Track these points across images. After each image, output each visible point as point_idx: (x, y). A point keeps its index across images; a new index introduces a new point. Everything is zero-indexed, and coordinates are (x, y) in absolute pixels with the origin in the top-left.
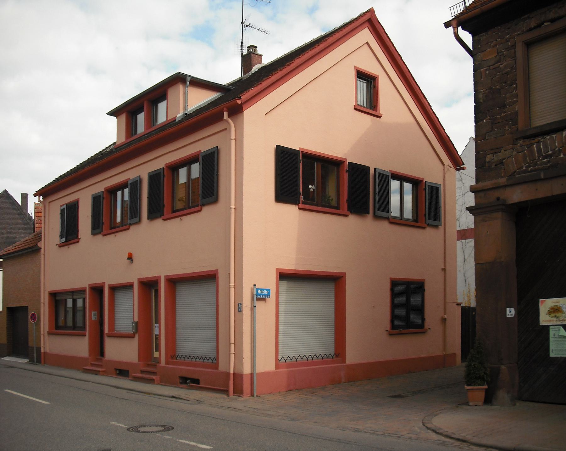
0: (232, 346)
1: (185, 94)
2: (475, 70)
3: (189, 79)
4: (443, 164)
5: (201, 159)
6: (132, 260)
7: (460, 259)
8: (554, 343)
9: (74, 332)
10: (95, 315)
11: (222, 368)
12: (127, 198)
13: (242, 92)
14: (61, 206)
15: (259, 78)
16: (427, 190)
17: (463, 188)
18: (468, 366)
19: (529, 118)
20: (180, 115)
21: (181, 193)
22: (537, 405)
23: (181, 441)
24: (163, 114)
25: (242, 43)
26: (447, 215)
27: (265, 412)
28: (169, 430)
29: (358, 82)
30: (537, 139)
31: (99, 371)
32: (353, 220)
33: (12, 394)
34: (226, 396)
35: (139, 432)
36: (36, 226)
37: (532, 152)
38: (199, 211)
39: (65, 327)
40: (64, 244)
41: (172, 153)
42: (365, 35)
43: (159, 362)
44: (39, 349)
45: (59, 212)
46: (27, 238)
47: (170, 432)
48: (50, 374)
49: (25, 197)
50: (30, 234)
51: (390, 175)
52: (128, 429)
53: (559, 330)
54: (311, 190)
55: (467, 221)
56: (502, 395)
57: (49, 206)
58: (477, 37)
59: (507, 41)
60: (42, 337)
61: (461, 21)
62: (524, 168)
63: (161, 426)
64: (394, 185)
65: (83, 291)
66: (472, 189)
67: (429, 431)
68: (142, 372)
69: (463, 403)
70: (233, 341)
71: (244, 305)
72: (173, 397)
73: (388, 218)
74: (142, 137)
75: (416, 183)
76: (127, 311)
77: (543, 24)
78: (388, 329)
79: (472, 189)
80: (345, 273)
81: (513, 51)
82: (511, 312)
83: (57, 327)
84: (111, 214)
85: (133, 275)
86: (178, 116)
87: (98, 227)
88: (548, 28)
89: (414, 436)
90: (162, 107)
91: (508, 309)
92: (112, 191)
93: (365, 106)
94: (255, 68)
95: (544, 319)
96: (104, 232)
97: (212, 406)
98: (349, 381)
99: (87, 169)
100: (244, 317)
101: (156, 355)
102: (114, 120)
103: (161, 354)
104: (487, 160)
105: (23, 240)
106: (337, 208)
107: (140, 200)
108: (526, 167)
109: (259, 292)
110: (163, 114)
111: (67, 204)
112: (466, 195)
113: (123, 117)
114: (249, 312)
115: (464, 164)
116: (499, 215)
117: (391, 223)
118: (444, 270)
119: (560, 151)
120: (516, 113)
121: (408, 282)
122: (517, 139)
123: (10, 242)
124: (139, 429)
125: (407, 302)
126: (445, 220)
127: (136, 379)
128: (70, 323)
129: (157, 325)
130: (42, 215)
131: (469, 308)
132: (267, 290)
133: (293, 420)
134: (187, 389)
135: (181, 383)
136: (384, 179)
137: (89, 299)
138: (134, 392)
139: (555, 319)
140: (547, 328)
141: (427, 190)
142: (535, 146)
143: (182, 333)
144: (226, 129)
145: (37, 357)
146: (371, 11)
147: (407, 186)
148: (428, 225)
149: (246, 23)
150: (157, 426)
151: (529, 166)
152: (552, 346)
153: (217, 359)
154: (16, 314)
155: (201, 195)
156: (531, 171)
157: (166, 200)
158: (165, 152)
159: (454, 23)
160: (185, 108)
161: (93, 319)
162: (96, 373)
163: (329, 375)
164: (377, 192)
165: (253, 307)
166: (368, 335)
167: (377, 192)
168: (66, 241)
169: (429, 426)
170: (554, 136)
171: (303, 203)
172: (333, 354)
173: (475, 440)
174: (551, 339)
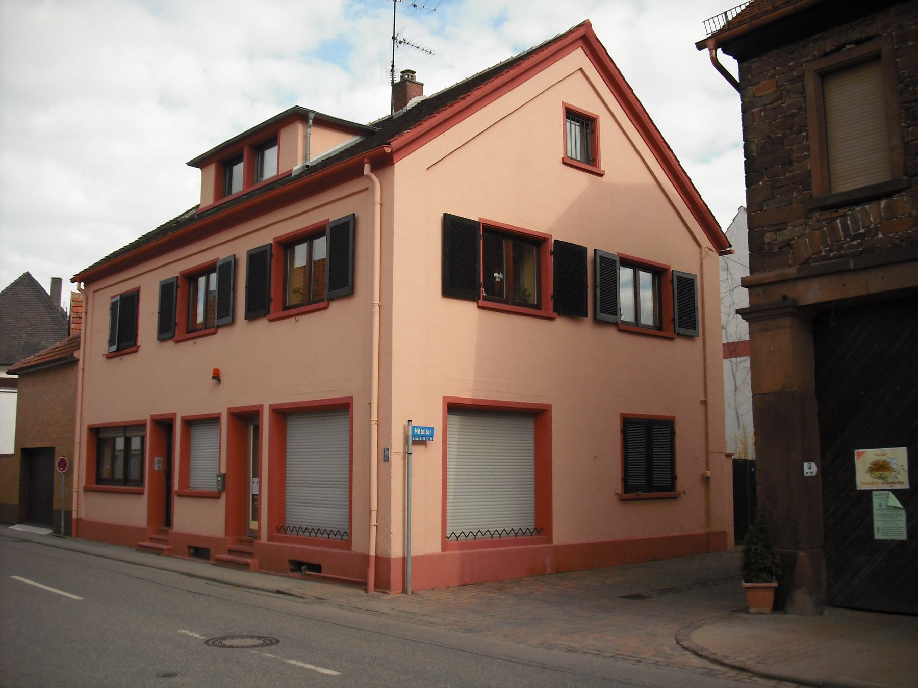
0: (374, 514)
1: (306, 137)
2: (744, 111)
3: (312, 116)
4: (699, 245)
5: (328, 232)
6: (219, 380)
7: (728, 386)
8: (880, 518)
9: (126, 487)
10: (159, 462)
11: (357, 547)
12: (213, 286)
13: (392, 136)
14: (112, 297)
15: (417, 116)
16: (675, 283)
17: (730, 280)
18: (747, 552)
19: (828, 180)
20: (297, 167)
21: (297, 282)
22: (857, 614)
23: (290, 662)
24: (272, 165)
25: (393, 66)
26: (707, 321)
27: (425, 618)
28: (271, 643)
29: (568, 124)
30: (841, 212)
31: (163, 550)
32: (561, 326)
33: (24, 583)
34: (362, 592)
35: (224, 646)
36: (73, 326)
37: (834, 229)
38: (325, 308)
39: (112, 480)
40: (115, 354)
41: (285, 222)
42: (578, 58)
43: (258, 537)
44: (69, 513)
45: (109, 306)
46: (58, 344)
47: (273, 647)
48: (85, 553)
49: (57, 283)
50: (63, 338)
51: (618, 260)
52: (206, 642)
53: (888, 497)
54: (498, 280)
55: (739, 330)
56: (801, 597)
57: (94, 296)
58: (745, 64)
59: (792, 69)
60: (75, 495)
61: (725, 40)
62: (823, 253)
63: (259, 637)
64: (625, 274)
65: (141, 426)
66: (745, 283)
67: (686, 652)
68: (231, 552)
69: (739, 608)
70: (374, 506)
71: (393, 451)
72: (279, 592)
73: (615, 324)
74: (240, 198)
75: (658, 272)
76: (209, 458)
77: (844, 47)
78: (619, 490)
79: (745, 283)
80: (550, 406)
81: (800, 84)
82: (810, 469)
83: (99, 480)
84: (189, 310)
85: (220, 403)
86: (295, 168)
87: (168, 329)
88: (852, 52)
89: (662, 660)
90: (271, 155)
91: (806, 464)
92: (191, 277)
93: (579, 158)
94: (413, 102)
95: (864, 480)
96: (177, 337)
97: (341, 606)
98: (558, 572)
99: (154, 243)
100: (393, 469)
101: (253, 525)
102: (198, 171)
103: (262, 525)
104: (767, 240)
105: (51, 347)
106: (538, 307)
107: (234, 291)
108: (826, 251)
109: (416, 431)
110: (272, 165)
111: (121, 295)
112: (736, 291)
113: (212, 169)
114: (401, 462)
115: (730, 246)
116: (787, 321)
117: (621, 331)
118: (704, 403)
119: (877, 230)
120: (809, 173)
121: (649, 420)
122: (810, 211)
123: (31, 349)
124: (224, 642)
125: (648, 452)
126: (704, 328)
127: (221, 563)
128: (119, 474)
129: (256, 480)
130: (83, 310)
131: (745, 461)
132: (429, 428)
133: (469, 631)
134: (301, 579)
135: (292, 571)
136: (609, 266)
137: (151, 437)
138: (216, 584)
139: (880, 481)
140: (868, 494)
141: (675, 283)
142: (838, 221)
143: (294, 493)
144: (367, 189)
145: (65, 525)
146: (586, 25)
147: (645, 277)
148: (679, 335)
149: (399, 39)
150: (252, 637)
151: (831, 251)
152: (878, 523)
153: (349, 533)
154: (34, 459)
155: (328, 285)
156: (835, 258)
157: (275, 291)
158: (274, 221)
159: (711, 43)
160: (306, 157)
161: (156, 468)
162: (158, 552)
163: (525, 562)
164: (598, 284)
165: (407, 454)
166: (587, 502)
167: (598, 284)
168: (118, 350)
169: (686, 644)
170: (867, 207)
171: (485, 299)
172: (532, 528)
173: (761, 668)
174: (876, 511)
